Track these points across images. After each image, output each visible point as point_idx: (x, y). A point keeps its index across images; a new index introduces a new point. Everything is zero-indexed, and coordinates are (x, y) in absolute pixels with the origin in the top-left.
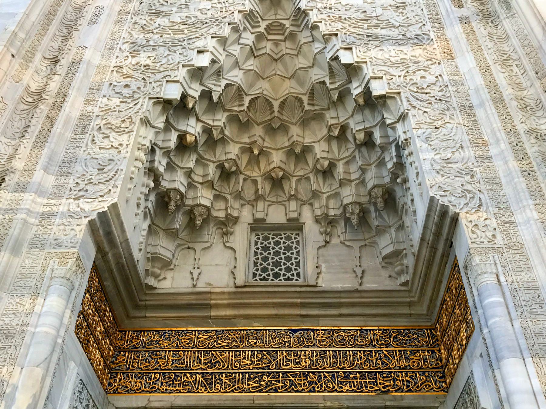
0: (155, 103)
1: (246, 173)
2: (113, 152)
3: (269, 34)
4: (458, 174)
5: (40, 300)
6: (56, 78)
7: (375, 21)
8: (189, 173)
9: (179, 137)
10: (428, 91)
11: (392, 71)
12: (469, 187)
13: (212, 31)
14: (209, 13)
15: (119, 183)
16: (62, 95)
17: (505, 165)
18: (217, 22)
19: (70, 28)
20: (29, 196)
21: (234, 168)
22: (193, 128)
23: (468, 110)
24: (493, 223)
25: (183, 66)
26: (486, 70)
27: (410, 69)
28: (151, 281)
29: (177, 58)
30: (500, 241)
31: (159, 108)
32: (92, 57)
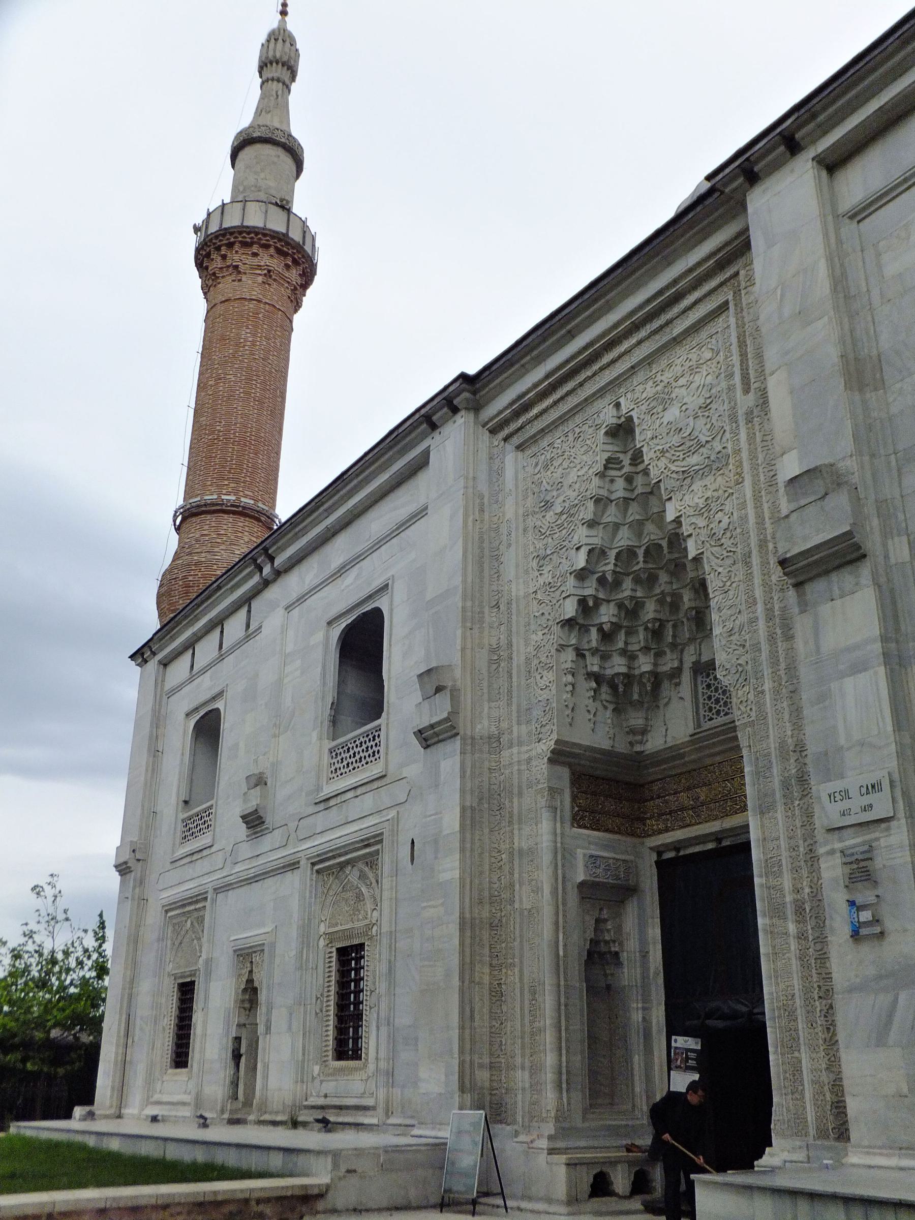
0: (562, 626)
1: (673, 618)
2: (547, 691)
3: (636, 465)
4: (736, 647)
5: (540, 825)
6: (502, 628)
7: (688, 444)
8: (624, 652)
9: (598, 630)
10: (723, 541)
11: (701, 522)
12: (739, 662)
13: (580, 518)
14: (577, 486)
15: (555, 720)
16: (510, 645)
19: (497, 558)
20: (515, 750)
21: (657, 625)
22: (607, 615)
24: (751, 696)
25: (571, 574)
26: (757, 498)
27: (712, 512)
28: (638, 748)
29: (565, 567)
30: (753, 714)
31: (566, 628)
32: (518, 589)
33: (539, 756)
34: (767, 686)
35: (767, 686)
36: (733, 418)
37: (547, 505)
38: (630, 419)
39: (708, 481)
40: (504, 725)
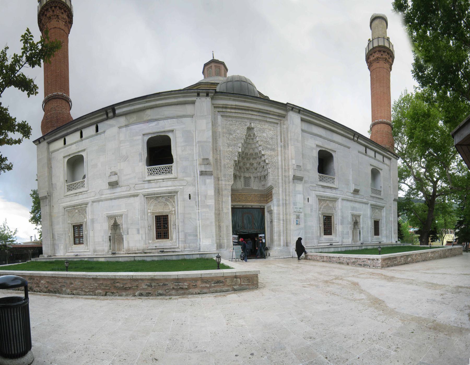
17: (280, 181)
18: (241, 139)
23: (278, 169)
26: (282, 161)
33: (228, 185)
34: (281, 189)
35: (281, 189)
36: (277, 144)
37: (230, 134)
38: (253, 128)
39: (272, 152)
40: (219, 176)
